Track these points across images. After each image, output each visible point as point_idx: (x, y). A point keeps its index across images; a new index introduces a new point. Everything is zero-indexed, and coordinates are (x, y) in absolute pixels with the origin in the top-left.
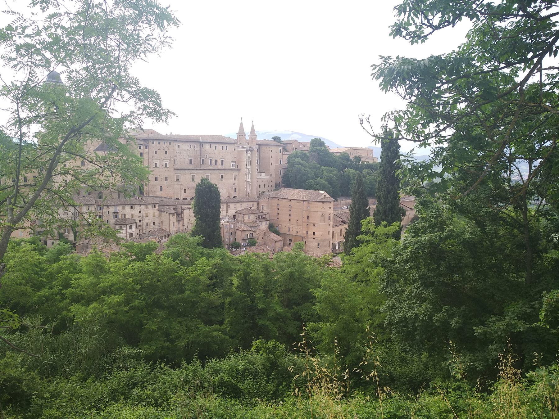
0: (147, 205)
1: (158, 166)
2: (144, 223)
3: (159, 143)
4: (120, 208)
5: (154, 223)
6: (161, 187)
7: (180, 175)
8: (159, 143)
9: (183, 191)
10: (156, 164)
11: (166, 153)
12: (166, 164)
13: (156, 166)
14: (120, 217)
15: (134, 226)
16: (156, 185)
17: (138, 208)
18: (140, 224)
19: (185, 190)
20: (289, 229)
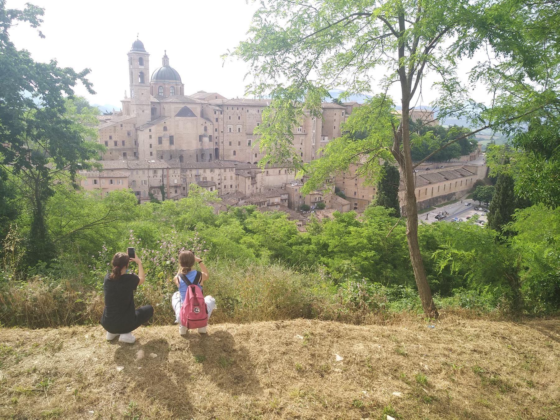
0: (225, 169)
1: (232, 131)
2: (223, 185)
3: (233, 109)
4: (201, 171)
5: (231, 186)
6: (235, 151)
7: (251, 139)
8: (233, 109)
9: (254, 156)
10: (230, 129)
11: (239, 119)
12: (239, 129)
13: (230, 131)
14: (201, 180)
15: (214, 188)
16: (230, 150)
17: (217, 171)
18: (219, 186)
19: (256, 155)
20: (355, 193)
